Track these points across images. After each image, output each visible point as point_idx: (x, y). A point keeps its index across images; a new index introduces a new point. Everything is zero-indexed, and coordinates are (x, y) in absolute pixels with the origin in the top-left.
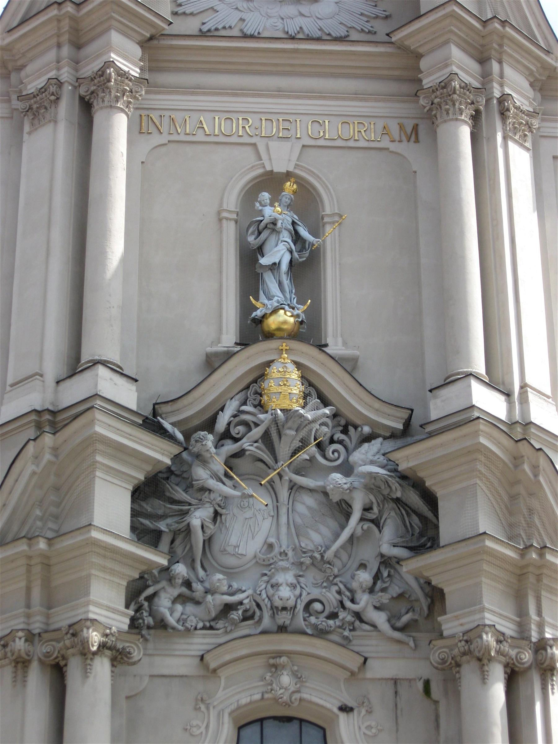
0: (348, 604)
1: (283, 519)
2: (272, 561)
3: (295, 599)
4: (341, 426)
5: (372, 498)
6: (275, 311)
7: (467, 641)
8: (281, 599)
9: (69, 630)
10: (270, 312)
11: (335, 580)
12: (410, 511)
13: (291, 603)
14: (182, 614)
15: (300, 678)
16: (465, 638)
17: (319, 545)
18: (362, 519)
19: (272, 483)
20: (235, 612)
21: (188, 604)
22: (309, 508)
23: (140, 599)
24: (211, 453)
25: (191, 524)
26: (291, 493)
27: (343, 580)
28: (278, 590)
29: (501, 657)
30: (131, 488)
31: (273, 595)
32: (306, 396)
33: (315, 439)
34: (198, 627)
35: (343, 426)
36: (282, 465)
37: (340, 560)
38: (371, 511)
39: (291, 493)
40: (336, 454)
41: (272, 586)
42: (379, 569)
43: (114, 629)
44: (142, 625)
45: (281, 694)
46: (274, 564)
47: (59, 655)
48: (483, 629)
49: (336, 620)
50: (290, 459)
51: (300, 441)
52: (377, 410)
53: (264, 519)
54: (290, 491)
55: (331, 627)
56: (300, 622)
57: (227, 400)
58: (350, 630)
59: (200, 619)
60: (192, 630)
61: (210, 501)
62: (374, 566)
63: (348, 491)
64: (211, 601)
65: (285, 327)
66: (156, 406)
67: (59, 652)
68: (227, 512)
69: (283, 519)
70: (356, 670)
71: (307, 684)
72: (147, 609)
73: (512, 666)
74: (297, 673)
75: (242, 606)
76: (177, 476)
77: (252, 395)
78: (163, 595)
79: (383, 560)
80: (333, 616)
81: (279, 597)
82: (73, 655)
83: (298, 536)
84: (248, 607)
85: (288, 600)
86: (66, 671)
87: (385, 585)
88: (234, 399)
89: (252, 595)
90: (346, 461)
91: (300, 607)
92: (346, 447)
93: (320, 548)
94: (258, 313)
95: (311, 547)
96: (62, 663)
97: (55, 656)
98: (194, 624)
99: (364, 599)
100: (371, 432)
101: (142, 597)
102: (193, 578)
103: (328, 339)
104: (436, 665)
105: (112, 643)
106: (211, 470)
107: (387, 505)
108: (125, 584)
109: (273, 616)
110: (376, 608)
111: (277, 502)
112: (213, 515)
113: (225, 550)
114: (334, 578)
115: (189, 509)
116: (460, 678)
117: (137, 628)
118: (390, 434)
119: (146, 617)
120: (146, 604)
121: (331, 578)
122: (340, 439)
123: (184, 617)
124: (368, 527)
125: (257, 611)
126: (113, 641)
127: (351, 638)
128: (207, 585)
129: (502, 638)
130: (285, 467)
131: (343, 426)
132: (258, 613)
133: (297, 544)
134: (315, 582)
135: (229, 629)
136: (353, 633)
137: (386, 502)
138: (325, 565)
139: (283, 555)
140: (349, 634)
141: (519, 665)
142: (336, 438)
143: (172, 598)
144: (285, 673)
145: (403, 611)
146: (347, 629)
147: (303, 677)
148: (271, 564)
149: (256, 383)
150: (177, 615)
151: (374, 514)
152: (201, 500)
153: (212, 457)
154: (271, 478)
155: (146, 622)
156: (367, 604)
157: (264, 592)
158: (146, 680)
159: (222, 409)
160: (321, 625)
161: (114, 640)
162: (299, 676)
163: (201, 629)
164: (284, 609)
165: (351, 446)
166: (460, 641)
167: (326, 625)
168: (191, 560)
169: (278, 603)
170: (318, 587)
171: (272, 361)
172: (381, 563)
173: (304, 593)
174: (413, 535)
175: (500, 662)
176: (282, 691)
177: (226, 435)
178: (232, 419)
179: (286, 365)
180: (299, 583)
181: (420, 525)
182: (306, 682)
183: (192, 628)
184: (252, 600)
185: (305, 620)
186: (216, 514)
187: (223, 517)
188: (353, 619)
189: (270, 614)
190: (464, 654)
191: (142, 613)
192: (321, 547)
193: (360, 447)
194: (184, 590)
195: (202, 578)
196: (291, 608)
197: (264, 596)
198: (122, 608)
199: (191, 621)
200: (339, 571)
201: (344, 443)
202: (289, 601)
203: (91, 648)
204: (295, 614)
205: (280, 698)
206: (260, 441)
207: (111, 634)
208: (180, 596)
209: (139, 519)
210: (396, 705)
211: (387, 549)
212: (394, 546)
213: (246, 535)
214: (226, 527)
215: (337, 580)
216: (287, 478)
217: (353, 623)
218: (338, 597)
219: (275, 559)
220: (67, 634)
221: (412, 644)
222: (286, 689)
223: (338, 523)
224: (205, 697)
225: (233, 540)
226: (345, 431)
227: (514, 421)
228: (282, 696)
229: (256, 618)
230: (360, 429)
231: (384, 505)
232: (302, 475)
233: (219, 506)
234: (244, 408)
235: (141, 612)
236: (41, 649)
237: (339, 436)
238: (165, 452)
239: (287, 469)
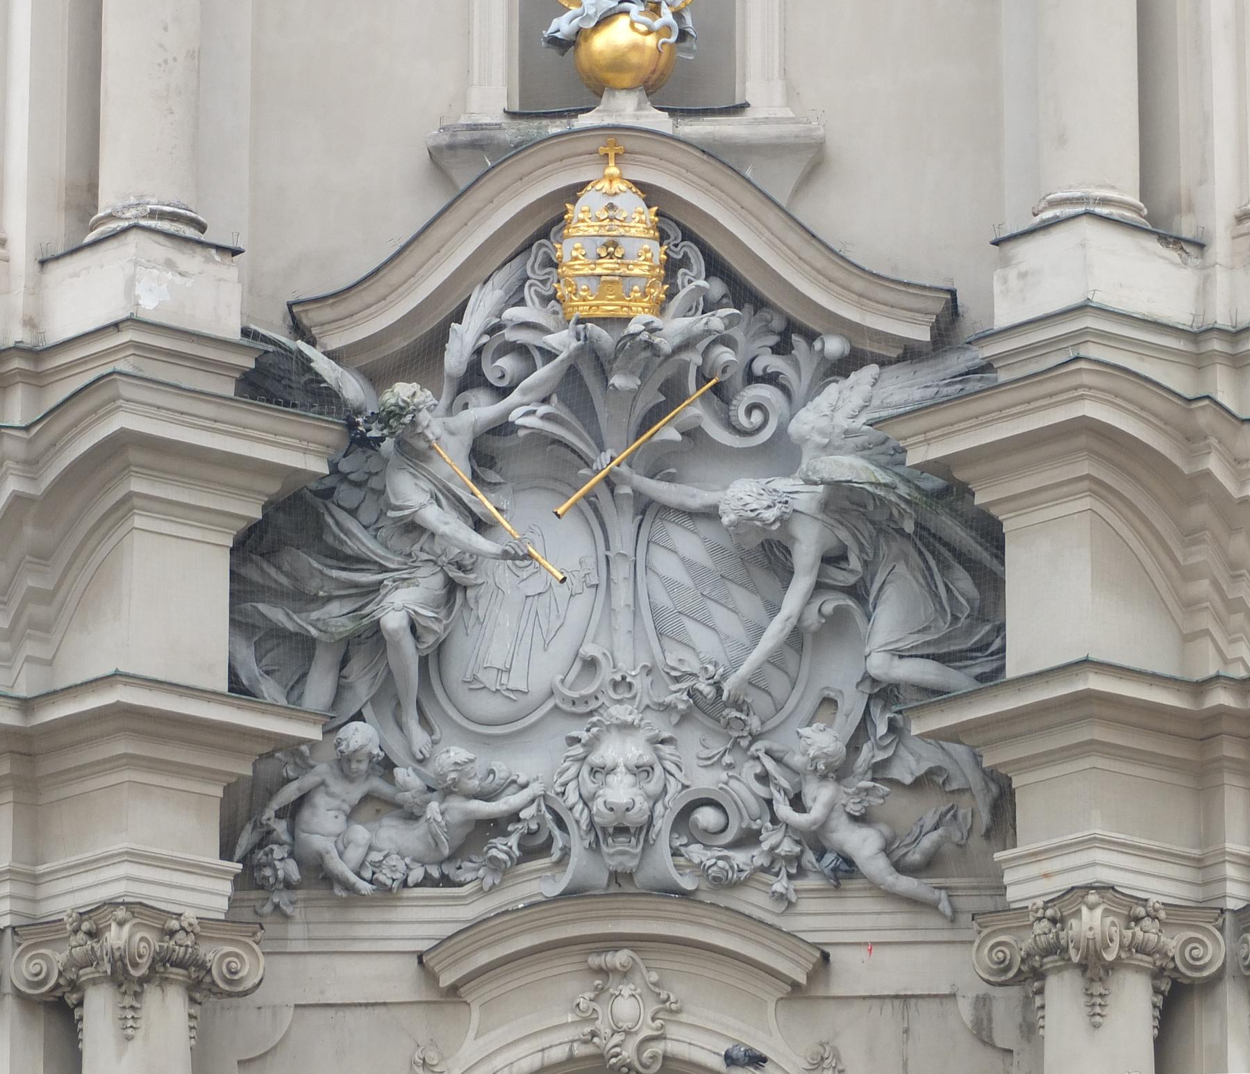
0: (784, 810)
1: (623, 594)
2: (594, 705)
3: (646, 806)
4: (773, 332)
5: (844, 535)
6: (606, 19)
7: (1053, 921)
8: (612, 809)
9: (81, 922)
10: (593, 24)
11: (753, 749)
12: (947, 554)
13: (637, 816)
14: (371, 848)
15: (664, 1002)
16: (1049, 913)
17: (710, 663)
18: (820, 587)
19: (593, 499)
20: (498, 842)
21: (386, 821)
22: (688, 564)
23: (265, 817)
24: (429, 441)
25: (381, 622)
26: (642, 521)
27: (775, 746)
28: (604, 784)
29: (1139, 956)
30: (230, 543)
31: (594, 797)
32: (672, 267)
33: (702, 378)
34: (411, 881)
35: (780, 334)
36: (612, 459)
37: (770, 695)
38: (843, 565)
39: (642, 521)
40: (757, 417)
41: (594, 771)
42: (867, 712)
43: (190, 915)
44: (272, 880)
45: (615, 1046)
46: (601, 711)
47: (62, 981)
48: (1083, 897)
49: (755, 852)
50: (637, 439)
51: (660, 390)
52: (861, 295)
53: (571, 595)
54: (640, 517)
55: (741, 871)
56: (662, 864)
57: (472, 288)
58: (790, 877)
59: (414, 860)
60: (395, 891)
61: (432, 558)
62: (853, 704)
63: (777, 525)
64: (439, 818)
65: (634, 58)
66: (295, 309)
67: (60, 974)
68: (480, 581)
69: (623, 594)
70: (802, 979)
71: (683, 1017)
72: (285, 837)
73: (1175, 975)
74: (657, 990)
75: (519, 826)
76: (358, 485)
77: (538, 272)
78: (320, 800)
79: (876, 690)
80: (749, 839)
81: (605, 802)
82: (94, 982)
83: (660, 635)
84: (534, 827)
85: (628, 810)
86: (81, 1019)
87: (880, 756)
88: (490, 283)
89: (545, 796)
90: (781, 431)
91: (663, 824)
92: (785, 390)
93: (711, 668)
94: (563, 25)
95: (693, 665)
96: (72, 999)
97: (52, 983)
98: (398, 876)
99: (820, 796)
100: (847, 352)
101: (270, 813)
102: (398, 752)
103: (748, 84)
104: (986, 976)
105: (186, 953)
106: (433, 479)
107: (885, 548)
108: (219, 792)
109: (595, 848)
110: (855, 819)
111: (608, 548)
112: (443, 592)
113: (475, 679)
114: (751, 744)
115: (381, 582)
116: (1043, 1007)
117: (262, 887)
118: (901, 351)
119: (282, 860)
120: (281, 827)
121: (744, 743)
122: (769, 371)
123: (375, 856)
124: (838, 609)
125: (557, 832)
126: (187, 946)
127: (793, 898)
128: (429, 771)
129: (1141, 911)
130: (618, 465)
131: (780, 334)
132: (559, 842)
133: (659, 657)
134: (705, 754)
135: (488, 881)
136: (800, 884)
137: (882, 540)
138: (727, 711)
139: (620, 690)
140: (787, 889)
141: (1189, 973)
142: (758, 368)
143: (347, 808)
144: (626, 990)
145: (930, 820)
146: (783, 872)
147: (672, 998)
148: (591, 713)
149: (549, 239)
150: (354, 854)
151: (852, 571)
152: (410, 555)
153: (431, 448)
154: (591, 489)
155: (281, 874)
156: (831, 808)
157: (572, 786)
158: (289, 1014)
159: (458, 316)
160: (714, 869)
161: (189, 943)
162: (663, 996)
163: (417, 885)
164: (621, 830)
165: (799, 386)
166: (1039, 919)
167: (727, 867)
168: (394, 703)
169: (604, 818)
170: (712, 764)
171: (583, 186)
172: (870, 697)
173: (673, 787)
174: (955, 618)
175: (1139, 969)
176: (617, 1038)
177: (473, 378)
178: (486, 339)
179: (615, 201)
180: (660, 759)
181: (974, 592)
182: (678, 1011)
183: (395, 885)
184: (543, 808)
185: (676, 853)
186: (452, 587)
187: (470, 593)
188: (797, 849)
189: (586, 843)
190: (1050, 950)
191: (272, 851)
192: (716, 664)
193: (819, 393)
194: (378, 784)
195: (421, 752)
196: (641, 828)
197: (572, 797)
198: (212, 858)
199: (393, 869)
200: (763, 723)
201: (781, 380)
202: (629, 813)
203: (132, 971)
204: (652, 842)
205: (612, 1057)
206: (554, 398)
207: (183, 928)
208: (367, 798)
209: (261, 607)
210: (905, 1064)
211: (879, 665)
212: (901, 657)
213: (527, 640)
214: (478, 618)
215: (760, 745)
216: (625, 490)
217: (798, 858)
218: (761, 790)
219: (602, 699)
220: (76, 932)
221: (944, 906)
222: (628, 1033)
223: (763, 598)
224: (432, 1057)
225: (497, 654)
226: (782, 348)
227: (1209, 322)
228: (618, 1050)
229: (556, 854)
230: (817, 345)
231: (876, 550)
232: (671, 479)
233: (460, 567)
234: (515, 313)
235: (267, 849)
237: (768, 362)
238: (312, 446)
239: (624, 469)
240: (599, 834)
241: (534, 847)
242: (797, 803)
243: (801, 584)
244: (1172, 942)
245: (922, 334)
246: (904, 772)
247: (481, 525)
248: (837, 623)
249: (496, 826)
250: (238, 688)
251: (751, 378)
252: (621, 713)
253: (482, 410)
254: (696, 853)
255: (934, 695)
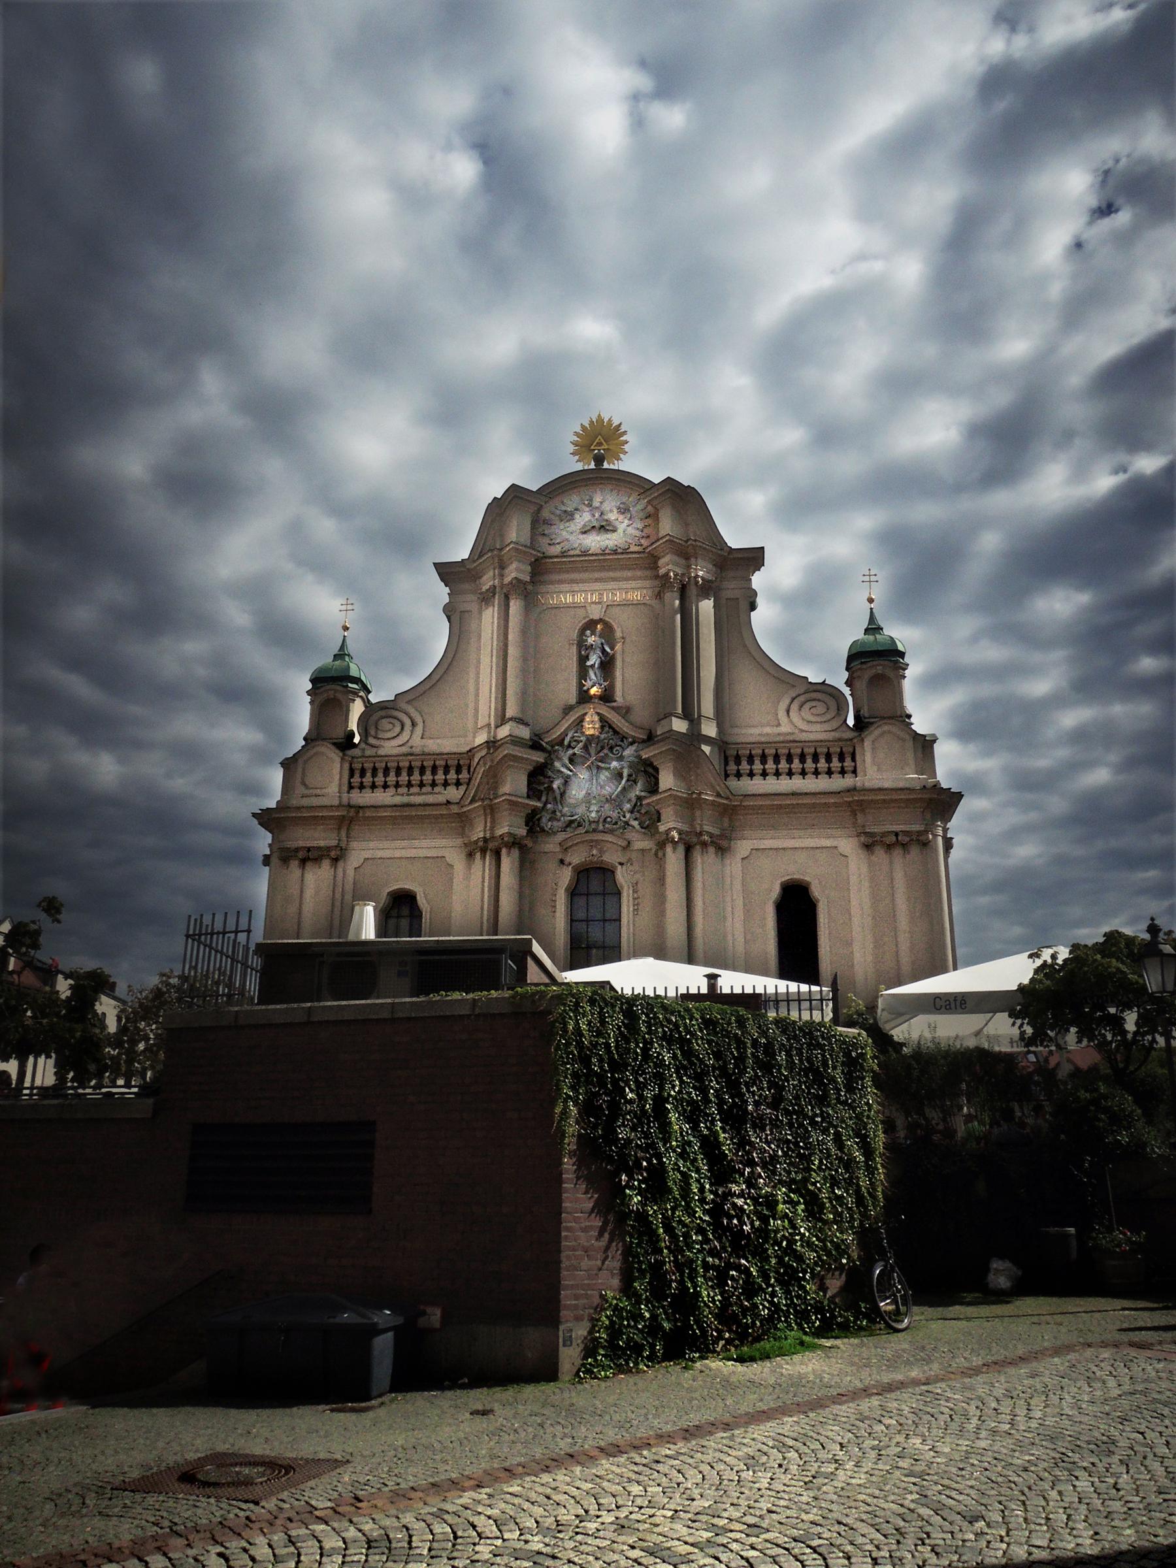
6: (592, 686)
18: (628, 780)
62: (634, 800)
80: (616, 823)
91: (601, 820)
94: (585, 688)
99: (628, 815)
177: (569, 746)
186: (566, 782)
211: (637, 793)
225: (574, 792)
226: (622, 741)
236: (491, 845)
240: (590, 823)
241: (580, 825)
242: (624, 817)
243: (623, 782)
244: (687, 838)
245: (645, 737)
246: (643, 811)
247: (571, 771)
248: (631, 786)
249: (572, 822)
250: (528, 797)
251: (617, 746)
252: (594, 802)
253: (570, 752)
254: (607, 826)
255: (645, 797)
